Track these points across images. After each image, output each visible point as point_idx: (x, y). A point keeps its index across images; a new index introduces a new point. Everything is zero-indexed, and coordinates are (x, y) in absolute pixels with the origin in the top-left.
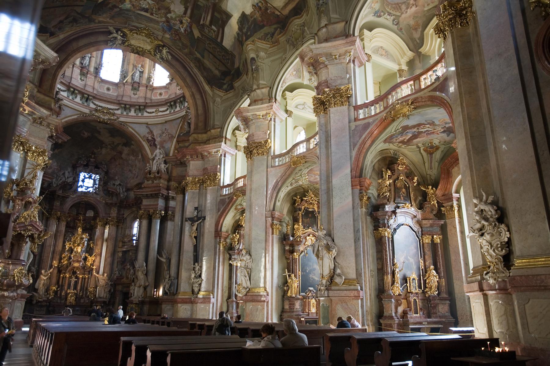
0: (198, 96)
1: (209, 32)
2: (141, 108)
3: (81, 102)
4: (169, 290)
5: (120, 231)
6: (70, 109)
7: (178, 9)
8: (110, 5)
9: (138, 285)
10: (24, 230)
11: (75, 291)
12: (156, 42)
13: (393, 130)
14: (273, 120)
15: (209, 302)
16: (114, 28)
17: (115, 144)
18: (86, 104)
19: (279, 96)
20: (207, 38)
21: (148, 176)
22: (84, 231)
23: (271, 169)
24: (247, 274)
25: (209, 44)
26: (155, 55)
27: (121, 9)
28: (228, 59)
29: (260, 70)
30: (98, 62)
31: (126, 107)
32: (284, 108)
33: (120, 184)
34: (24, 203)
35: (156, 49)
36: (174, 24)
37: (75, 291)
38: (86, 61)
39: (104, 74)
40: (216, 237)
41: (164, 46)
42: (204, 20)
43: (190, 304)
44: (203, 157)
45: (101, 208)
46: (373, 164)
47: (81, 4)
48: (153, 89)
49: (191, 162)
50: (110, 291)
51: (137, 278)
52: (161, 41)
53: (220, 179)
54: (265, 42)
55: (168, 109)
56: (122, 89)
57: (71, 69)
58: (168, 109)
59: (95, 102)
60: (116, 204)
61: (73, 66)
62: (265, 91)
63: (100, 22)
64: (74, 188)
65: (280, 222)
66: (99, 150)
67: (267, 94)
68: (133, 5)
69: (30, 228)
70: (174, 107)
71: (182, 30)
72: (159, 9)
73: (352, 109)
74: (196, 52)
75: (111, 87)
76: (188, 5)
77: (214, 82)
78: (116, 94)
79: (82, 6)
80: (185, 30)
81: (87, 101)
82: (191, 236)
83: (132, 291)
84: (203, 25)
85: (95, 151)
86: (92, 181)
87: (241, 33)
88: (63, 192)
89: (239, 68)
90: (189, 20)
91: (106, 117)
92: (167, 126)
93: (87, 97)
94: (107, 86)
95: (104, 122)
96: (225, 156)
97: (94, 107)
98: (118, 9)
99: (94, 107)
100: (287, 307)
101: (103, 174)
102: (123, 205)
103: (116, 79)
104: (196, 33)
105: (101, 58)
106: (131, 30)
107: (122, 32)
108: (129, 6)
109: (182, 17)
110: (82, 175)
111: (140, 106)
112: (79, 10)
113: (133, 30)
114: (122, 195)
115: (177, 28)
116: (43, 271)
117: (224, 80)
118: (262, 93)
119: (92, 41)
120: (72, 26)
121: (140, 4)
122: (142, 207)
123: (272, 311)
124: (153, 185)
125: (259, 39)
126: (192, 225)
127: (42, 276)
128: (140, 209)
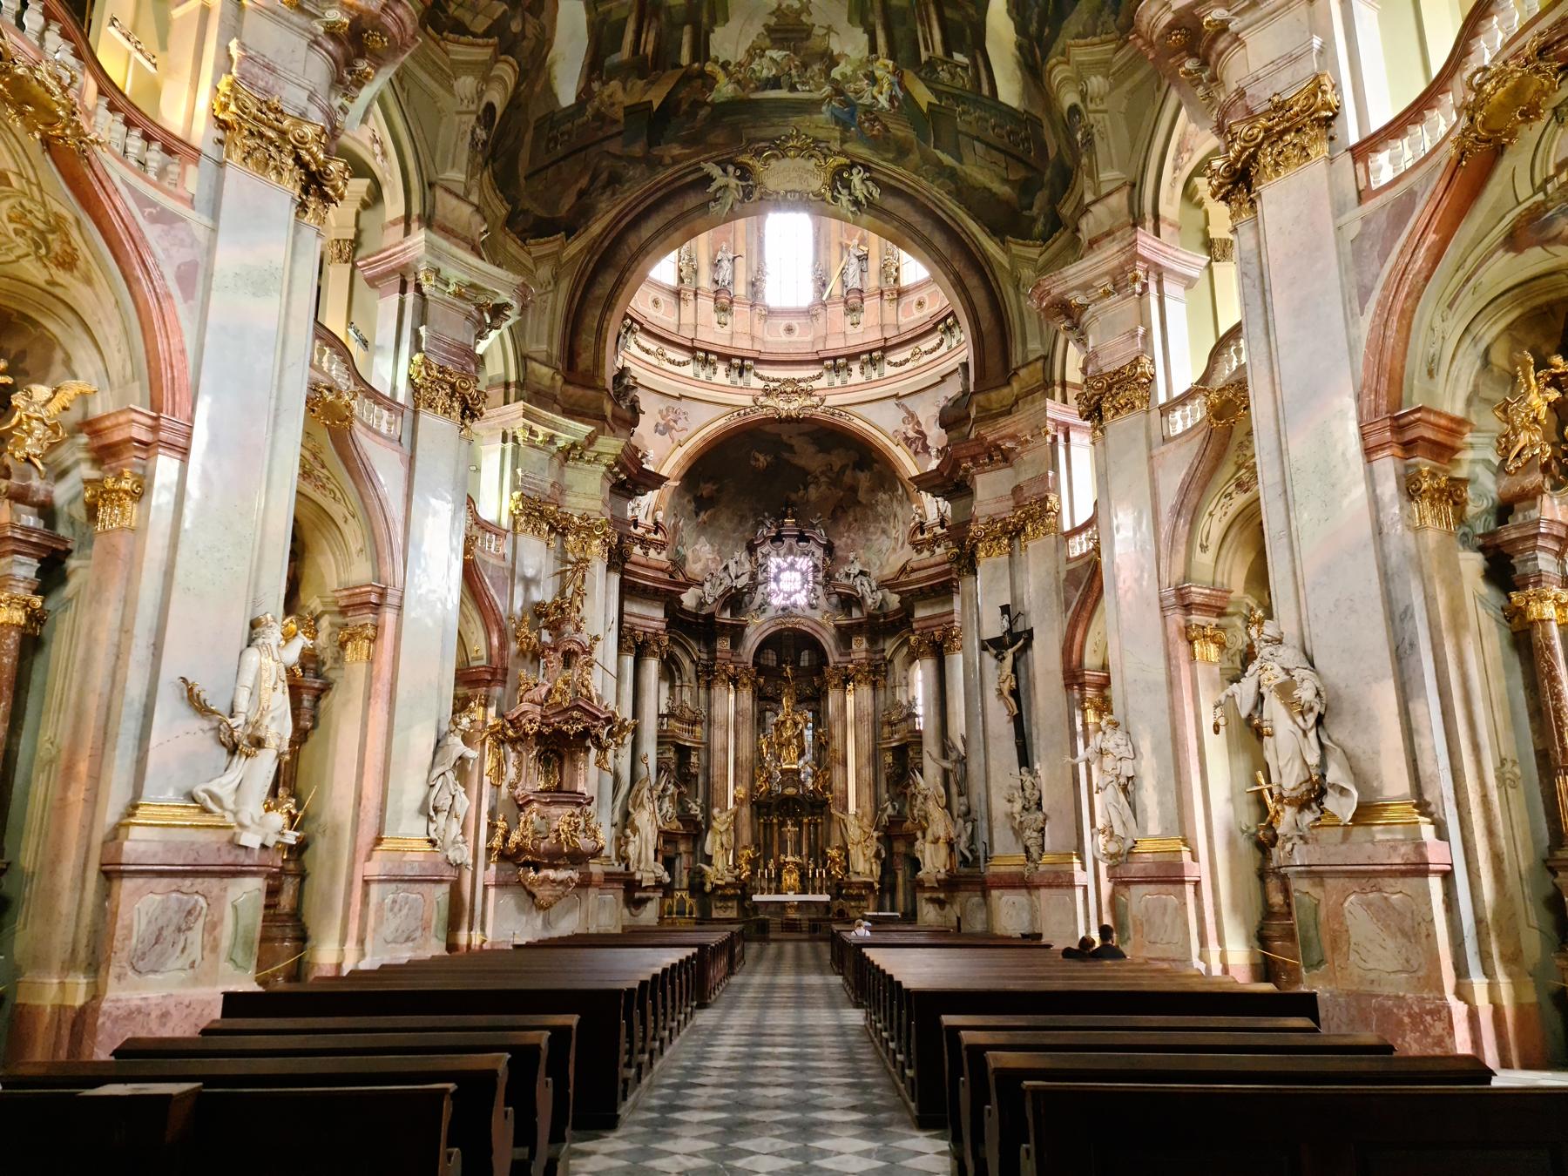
0: (972, 282)
1: (953, 76)
2: (874, 356)
3: (727, 382)
4: (971, 851)
5: (882, 697)
7: (850, 45)
8: (685, 107)
9: (929, 837)
10: (567, 722)
11: (798, 859)
12: (834, 162)
13: (1524, 190)
14: (1153, 287)
15: (1071, 885)
16: (718, 163)
17: (836, 469)
18: (740, 383)
19: (1170, 201)
20: (953, 96)
21: (920, 537)
22: (801, 700)
23: (1163, 448)
24: (1122, 796)
25: (964, 112)
26: (835, 199)
27: (714, 105)
28: (1027, 139)
29: (1097, 138)
30: (755, 268)
31: (838, 363)
32: (1199, 237)
33: (862, 573)
34: (559, 655)
35: (834, 180)
37: (798, 859)
38: (725, 273)
39: (774, 295)
40: (1068, 686)
41: (853, 165)
42: (927, 48)
43: (1024, 891)
44: (1007, 458)
45: (828, 640)
46: (1482, 346)
47: (615, 129)
48: (901, 293)
49: (978, 478)
50: (877, 855)
51: (926, 819)
52: (842, 153)
53: (1059, 513)
54: (1096, 40)
55: (942, 341)
56: (821, 320)
57: (691, 304)
58: (942, 341)
59: (761, 372)
60: (860, 625)
61: (696, 294)
62: (1119, 201)
64: (758, 599)
65: (1221, 613)
66: (801, 493)
67: (1126, 210)
68: (738, 82)
69: (575, 714)
70: (956, 331)
71: (883, 101)
73: (1347, 159)
74: (938, 152)
75: (794, 323)
76: (871, 18)
77: (1007, 222)
78: (809, 338)
79: (620, 133)
81: (741, 375)
82: (1000, 692)
83: (918, 855)
84: (931, 63)
85: (793, 497)
86: (798, 576)
87: (1025, 42)
88: (732, 615)
89: (1059, 153)
90: (890, 63)
91: (794, 406)
93: (739, 364)
94: (783, 323)
95: (789, 420)
96: (1067, 439)
97: (761, 384)
98: (708, 109)
99: (761, 384)
100: (1277, 899)
101: (819, 553)
102: (881, 626)
103: (804, 296)
104: (923, 96)
105: (761, 252)
106: (758, 153)
107: (738, 166)
108: (731, 87)
110: (774, 562)
111: (870, 352)
112: (614, 147)
114: (870, 601)
115: (867, 100)
116: (716, 811)
117: (1030, 207)
118: (1112, 213)
119: (671, 217)
120: (614, 194)
122: (915, 626)
123: (1217, 913)
124: (932, 561)
125: (1078, 36)
126: (1000, 658)
127: (714, 824)
128: (913, 632)
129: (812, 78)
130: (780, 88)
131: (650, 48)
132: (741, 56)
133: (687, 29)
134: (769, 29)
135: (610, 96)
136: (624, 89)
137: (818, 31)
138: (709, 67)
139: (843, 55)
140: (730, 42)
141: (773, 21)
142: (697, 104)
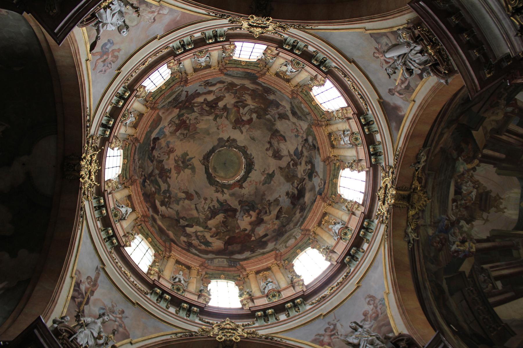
6: (103, 91)
25: (472, 291)
27: (455, 160)
36: (454, 233)
42: (491, 267)
63: (442, 134)
68: (463, 174)
71: (454, 247)
72: (466, 208)
74: (444, 282)
79: (478, 112)
80: (456, 251)
81: (103, 125)
90: (474, 250)
92: (130, 311)
104: (466, 267)
109: (471, 240)
113: (420, 183)
115: (451, 239)
121: (467, 182)
129: (460, 211)
130: (455, 195)
131: (504, 137)
132: (476, 178)
133: (503, 156)
134: (488, 193)
135: (497, 114)
136: (493, 120)
137: (485, 215)
138: (476, 161)
139: (472, 226)
140: (486, 175)
141: (493, 194)
142: (460, 151)
